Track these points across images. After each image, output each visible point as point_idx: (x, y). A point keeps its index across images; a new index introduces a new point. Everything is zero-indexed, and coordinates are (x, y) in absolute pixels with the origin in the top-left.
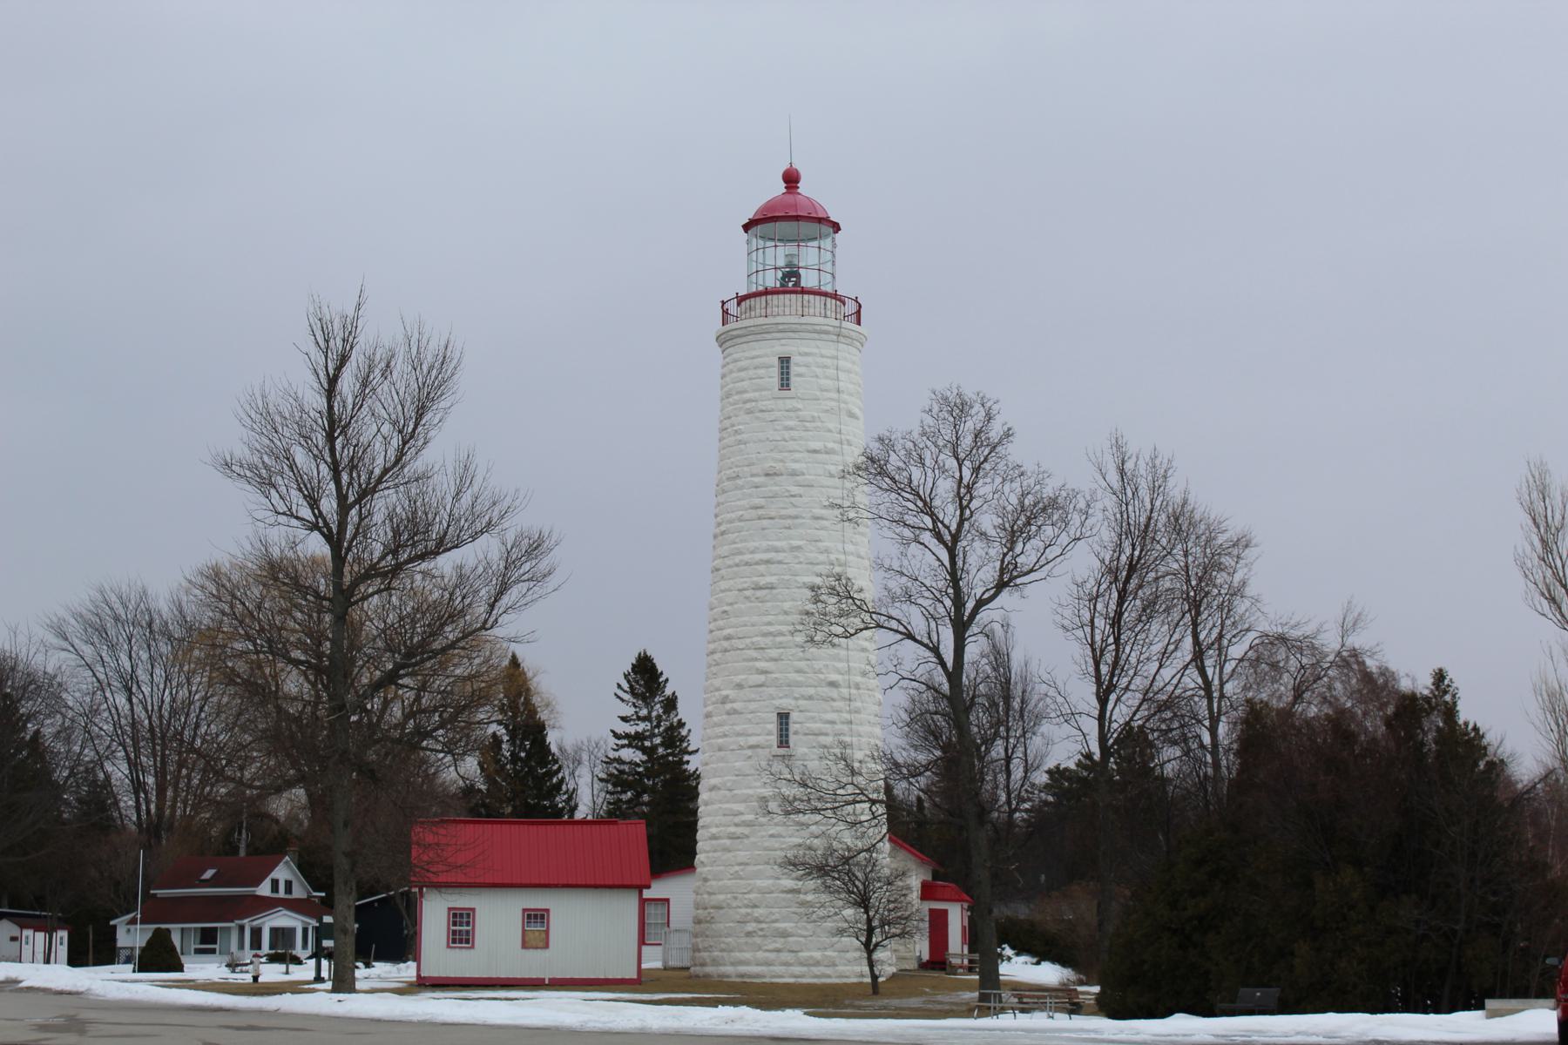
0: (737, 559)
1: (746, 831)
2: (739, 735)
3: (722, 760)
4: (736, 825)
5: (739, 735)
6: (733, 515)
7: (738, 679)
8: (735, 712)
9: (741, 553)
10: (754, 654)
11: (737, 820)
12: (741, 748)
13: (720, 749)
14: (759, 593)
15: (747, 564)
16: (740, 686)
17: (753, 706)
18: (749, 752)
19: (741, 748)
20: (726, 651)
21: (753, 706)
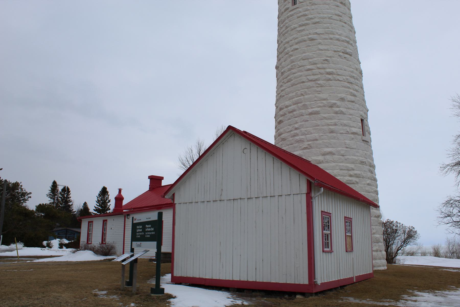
0: (332, 36)
1: (357, 180)
2: (345, 125)
3: (334, 138)
4: (351, 176)
5: (345, 125)
6: (325, 16)
7: (343, 95)
8: (342, 113)
9: (333, 34)
10: (348, 85)
11: (352, 173)
12: (348, 133)
13: (332, 132)
14: (346, 56)
15: (338, 40)
16: (342, 99)
17: (351, 112)
18: (352, 136)
19: (348, 133)
20: (330, 80)
21: (351, 112)
